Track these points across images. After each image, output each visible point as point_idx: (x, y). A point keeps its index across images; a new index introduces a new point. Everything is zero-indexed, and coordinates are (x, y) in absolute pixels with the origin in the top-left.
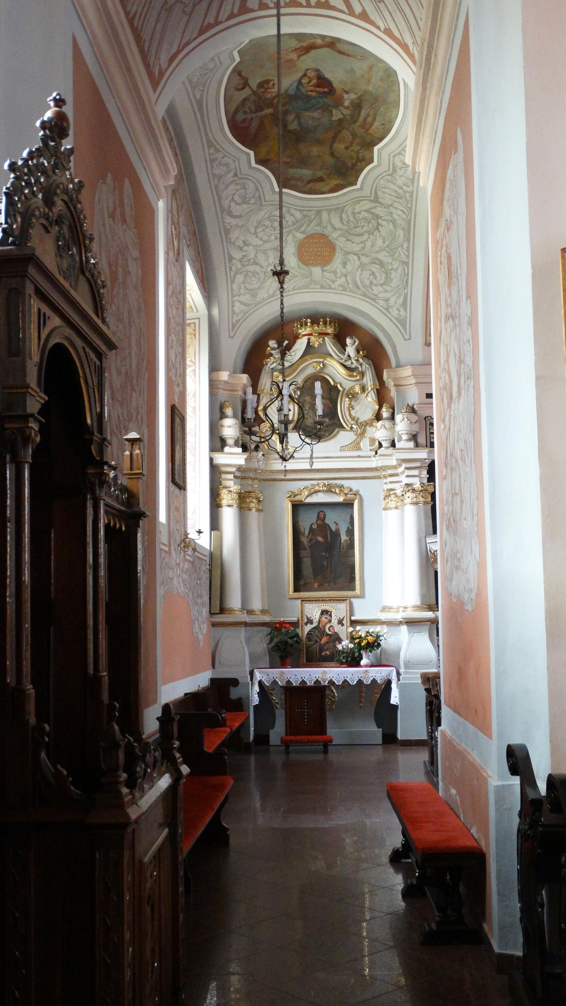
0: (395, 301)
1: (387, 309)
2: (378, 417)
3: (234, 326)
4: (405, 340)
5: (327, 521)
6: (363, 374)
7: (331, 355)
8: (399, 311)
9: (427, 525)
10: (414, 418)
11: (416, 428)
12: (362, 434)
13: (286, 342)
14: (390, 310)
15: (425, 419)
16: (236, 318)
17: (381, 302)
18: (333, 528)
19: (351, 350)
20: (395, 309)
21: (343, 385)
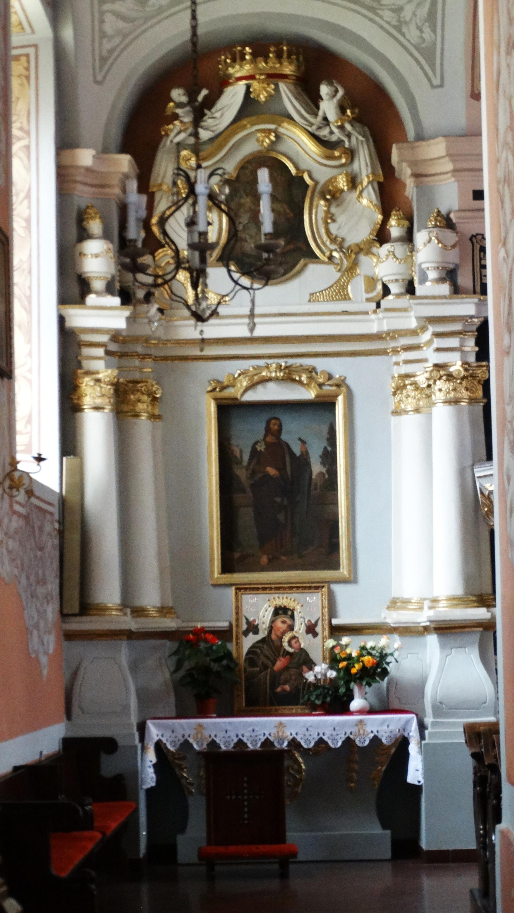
1: (398, 28)
2: (382, 236)
3: (103, 60)
4: (433, 87)
5: (284, 437)
6: (351, 154)
7: (290, 118)
8: (421, 31)
9: (475, 444)
10: (451, 237)
11: (453, 258)
12: (352, 269)
13: (204, 92)
14: (404, 29)
15: (471, 239)
16: (107, 46)
17: (387, 15)
18: (297, 450)
19: (328, 107)
20: (413, 27)
21: (315, 176)
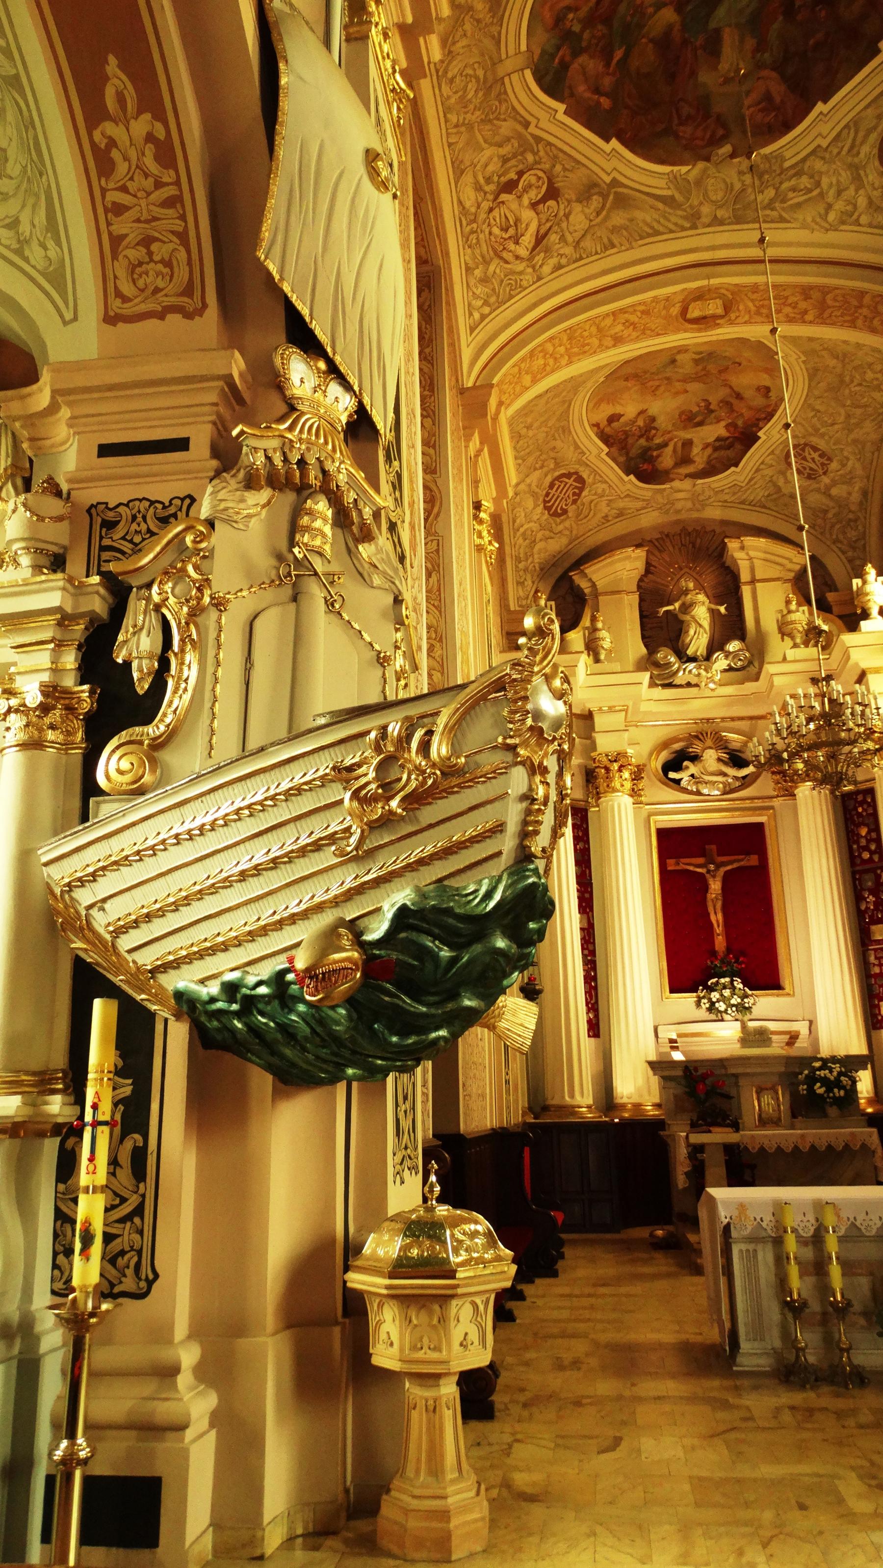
0: (32, 221)
1: (19, 252)
4: (65, 323)
8: (45, 249)
10: (56, 506)
14: (27, 253)
15: (89, 511)
20: (35, 245)
